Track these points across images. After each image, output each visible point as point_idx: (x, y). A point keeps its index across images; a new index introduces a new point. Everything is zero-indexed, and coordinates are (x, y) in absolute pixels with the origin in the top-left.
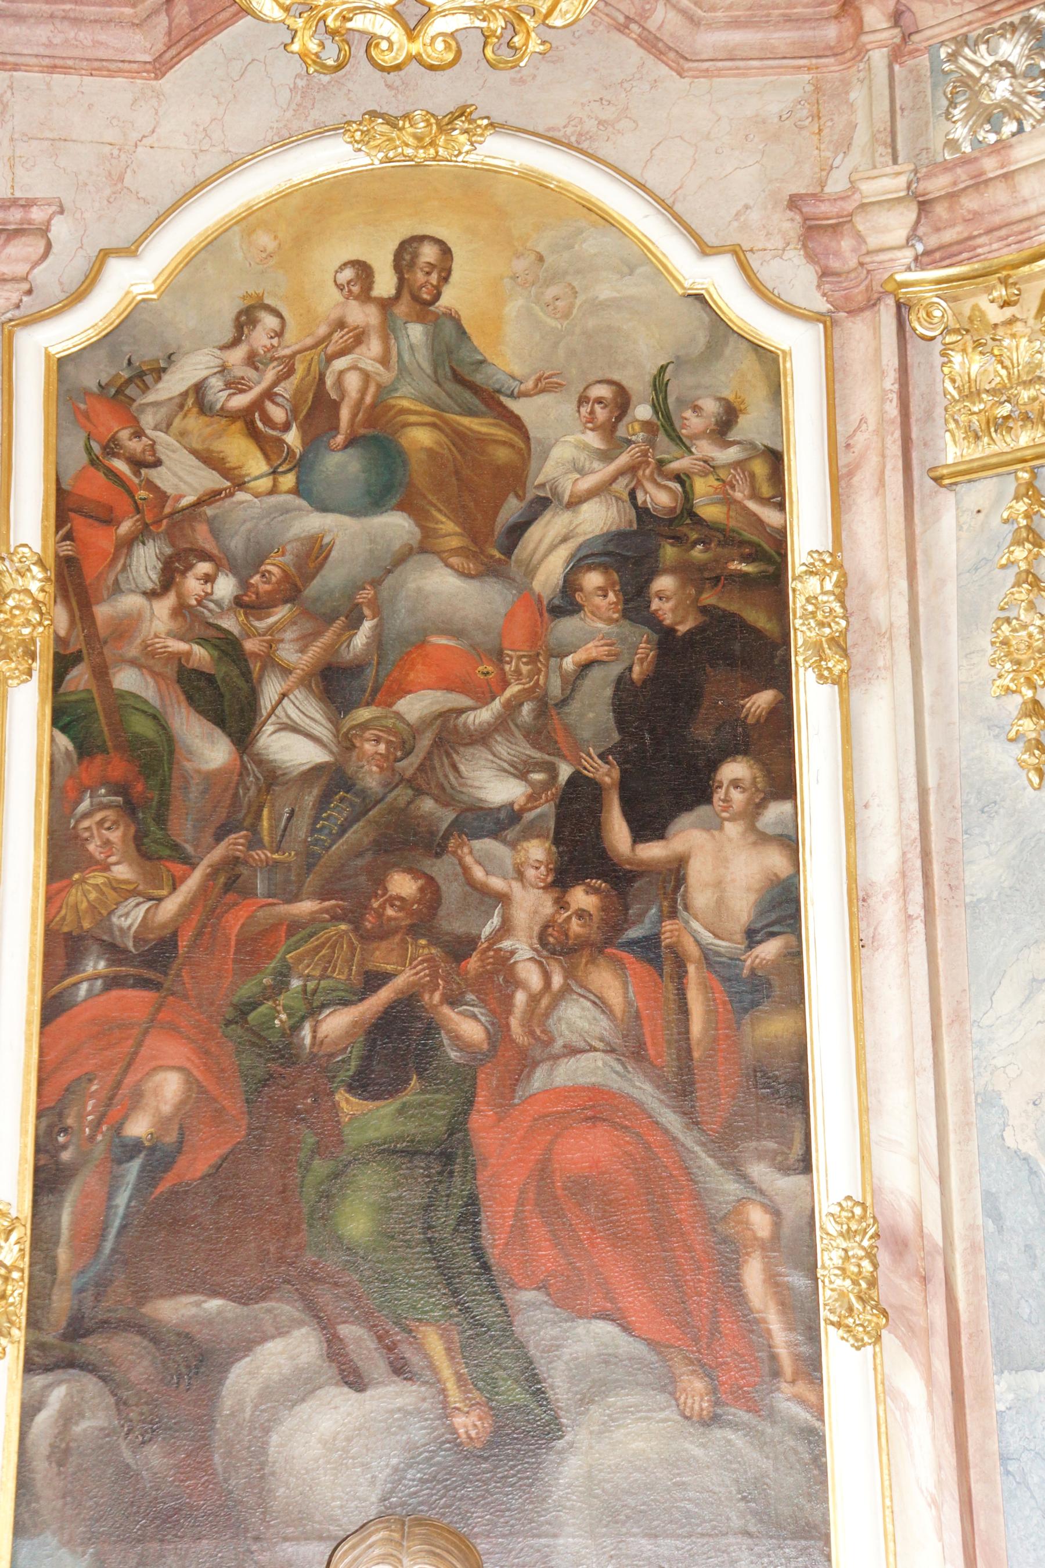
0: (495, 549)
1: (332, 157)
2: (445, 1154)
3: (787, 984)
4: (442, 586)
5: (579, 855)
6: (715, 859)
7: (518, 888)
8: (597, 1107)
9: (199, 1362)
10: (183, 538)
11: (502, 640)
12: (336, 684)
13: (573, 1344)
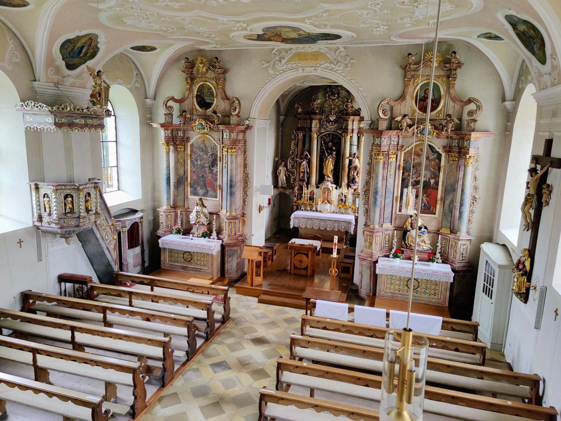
0: (207, 155)
1: (200, 135)
2: (205, 181)
3: (216, 175)
4: (205, 156)
5: (210, 169)
6: (214, 169)
7: (207, 169)
8: (210, 179)
9: (196, 188)
10: (194, 152)
11: (207, 158)
12: (200, 160)
13: (209, 189)
